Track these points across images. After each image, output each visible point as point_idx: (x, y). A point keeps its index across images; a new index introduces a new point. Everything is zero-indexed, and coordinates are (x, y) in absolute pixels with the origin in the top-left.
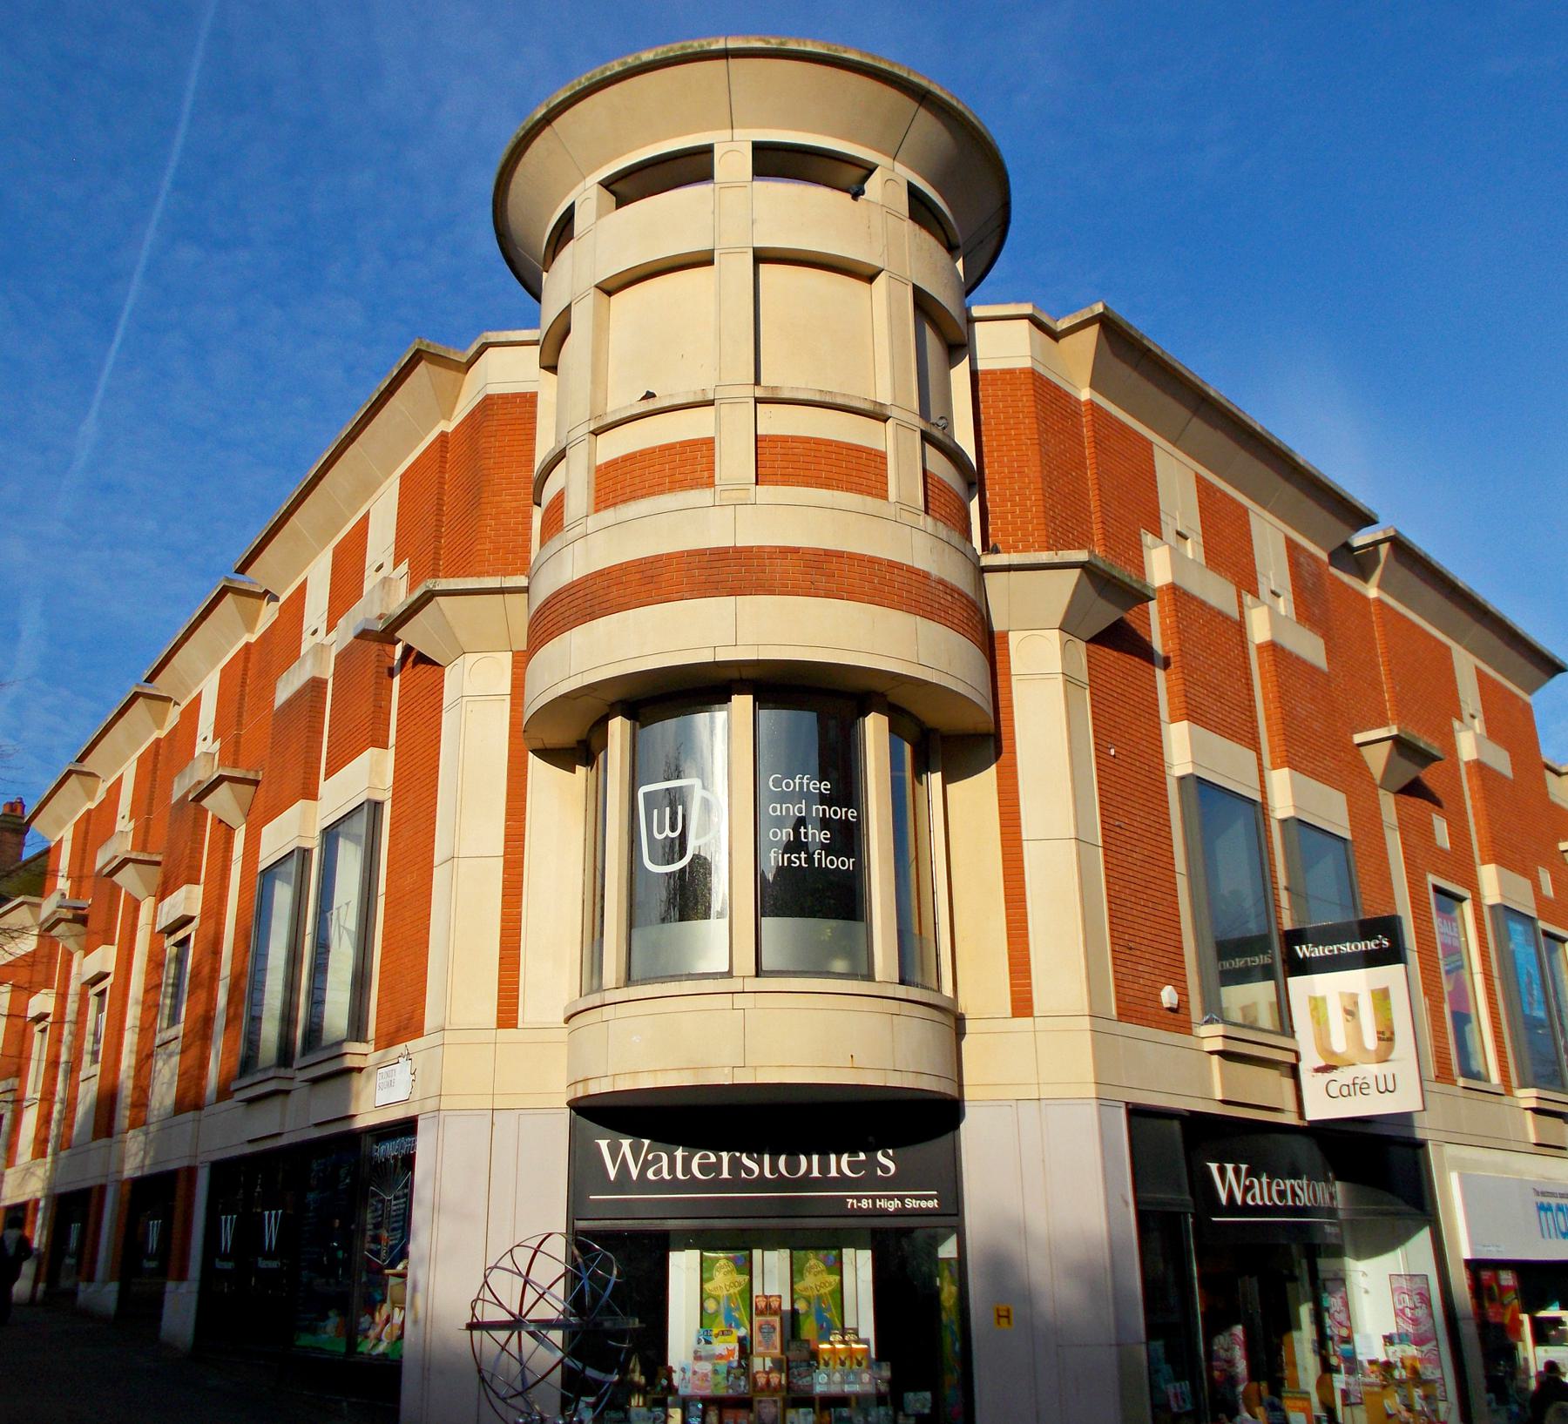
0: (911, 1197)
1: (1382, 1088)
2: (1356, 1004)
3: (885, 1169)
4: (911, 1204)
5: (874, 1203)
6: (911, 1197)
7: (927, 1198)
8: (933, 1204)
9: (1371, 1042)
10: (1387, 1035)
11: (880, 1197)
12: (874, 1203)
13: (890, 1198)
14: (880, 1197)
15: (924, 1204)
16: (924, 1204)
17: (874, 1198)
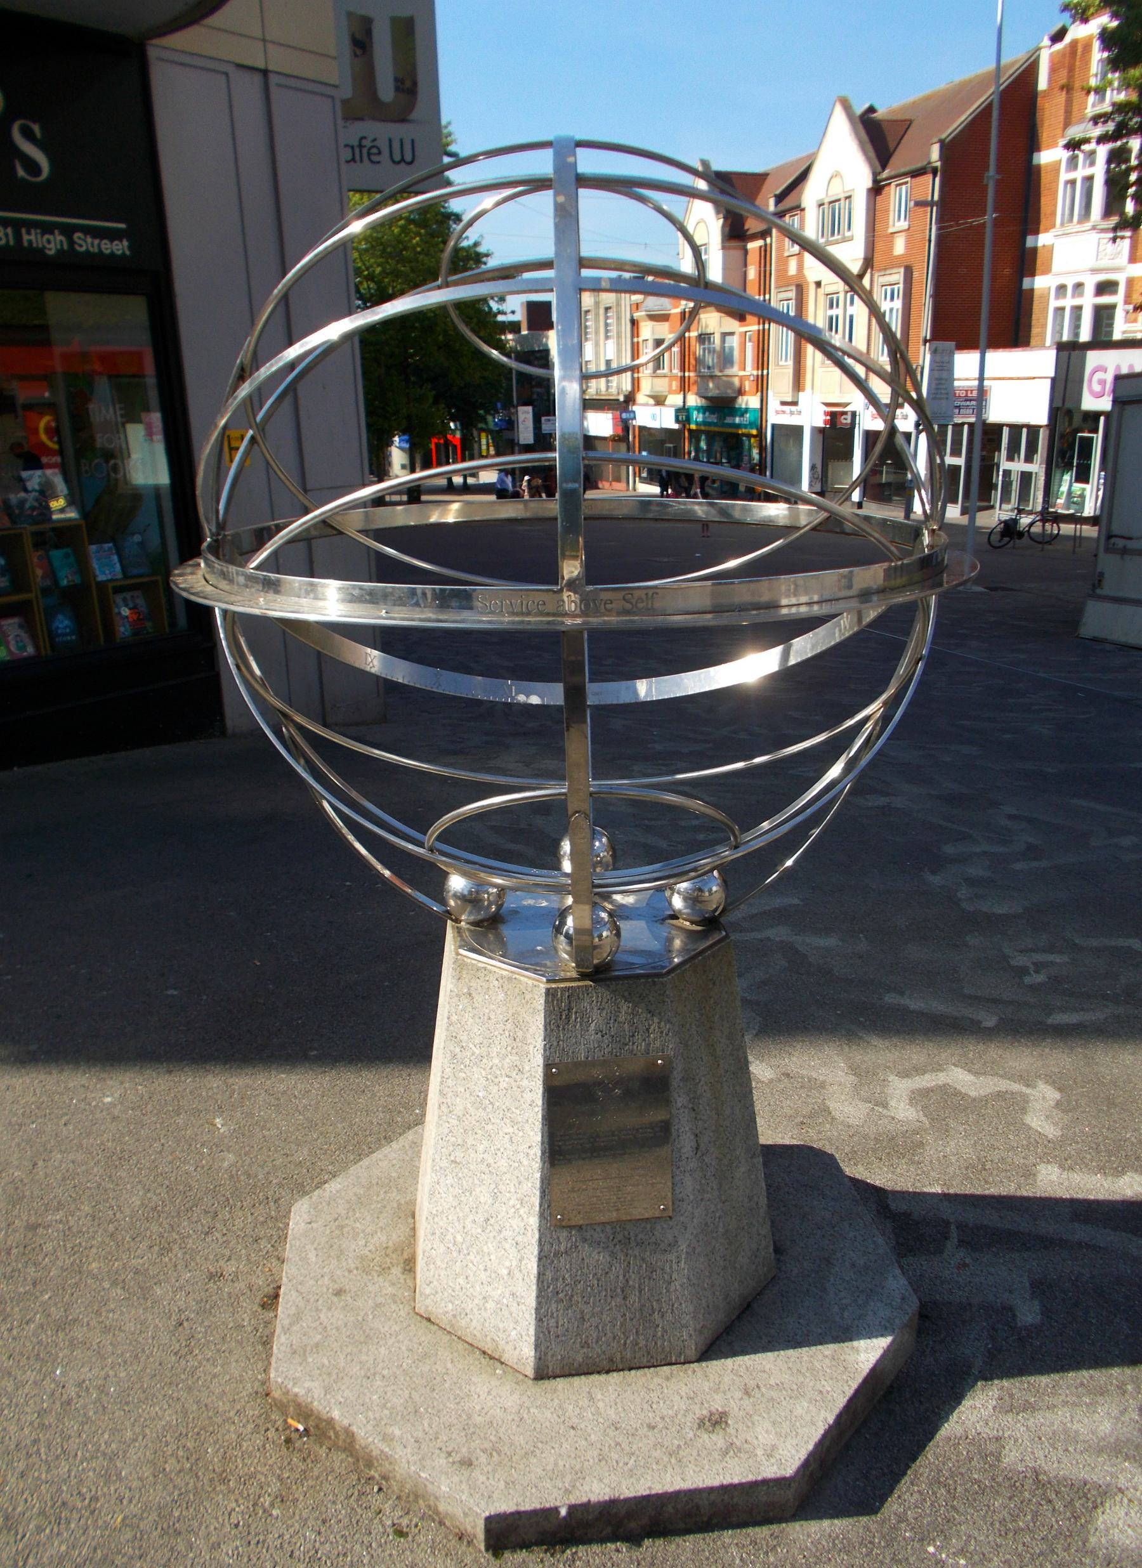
0: (87, 230)
1: (397, 157)
2: (369, 32)
3: (33, 167)
4: (85, 244)
5: (18, 237)
6: (87, 230)
7: (113, 235)
8: (120, 247)
9: (386, 91)
10: (408, 84)
11: (31, 225)
12: (18, 237)
13: (47, 228)
14: (31, 225)
15: (107, 247)
16: (107, 247)
17: (17, 225)
